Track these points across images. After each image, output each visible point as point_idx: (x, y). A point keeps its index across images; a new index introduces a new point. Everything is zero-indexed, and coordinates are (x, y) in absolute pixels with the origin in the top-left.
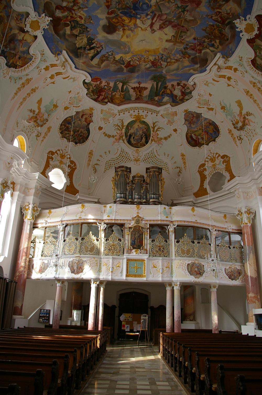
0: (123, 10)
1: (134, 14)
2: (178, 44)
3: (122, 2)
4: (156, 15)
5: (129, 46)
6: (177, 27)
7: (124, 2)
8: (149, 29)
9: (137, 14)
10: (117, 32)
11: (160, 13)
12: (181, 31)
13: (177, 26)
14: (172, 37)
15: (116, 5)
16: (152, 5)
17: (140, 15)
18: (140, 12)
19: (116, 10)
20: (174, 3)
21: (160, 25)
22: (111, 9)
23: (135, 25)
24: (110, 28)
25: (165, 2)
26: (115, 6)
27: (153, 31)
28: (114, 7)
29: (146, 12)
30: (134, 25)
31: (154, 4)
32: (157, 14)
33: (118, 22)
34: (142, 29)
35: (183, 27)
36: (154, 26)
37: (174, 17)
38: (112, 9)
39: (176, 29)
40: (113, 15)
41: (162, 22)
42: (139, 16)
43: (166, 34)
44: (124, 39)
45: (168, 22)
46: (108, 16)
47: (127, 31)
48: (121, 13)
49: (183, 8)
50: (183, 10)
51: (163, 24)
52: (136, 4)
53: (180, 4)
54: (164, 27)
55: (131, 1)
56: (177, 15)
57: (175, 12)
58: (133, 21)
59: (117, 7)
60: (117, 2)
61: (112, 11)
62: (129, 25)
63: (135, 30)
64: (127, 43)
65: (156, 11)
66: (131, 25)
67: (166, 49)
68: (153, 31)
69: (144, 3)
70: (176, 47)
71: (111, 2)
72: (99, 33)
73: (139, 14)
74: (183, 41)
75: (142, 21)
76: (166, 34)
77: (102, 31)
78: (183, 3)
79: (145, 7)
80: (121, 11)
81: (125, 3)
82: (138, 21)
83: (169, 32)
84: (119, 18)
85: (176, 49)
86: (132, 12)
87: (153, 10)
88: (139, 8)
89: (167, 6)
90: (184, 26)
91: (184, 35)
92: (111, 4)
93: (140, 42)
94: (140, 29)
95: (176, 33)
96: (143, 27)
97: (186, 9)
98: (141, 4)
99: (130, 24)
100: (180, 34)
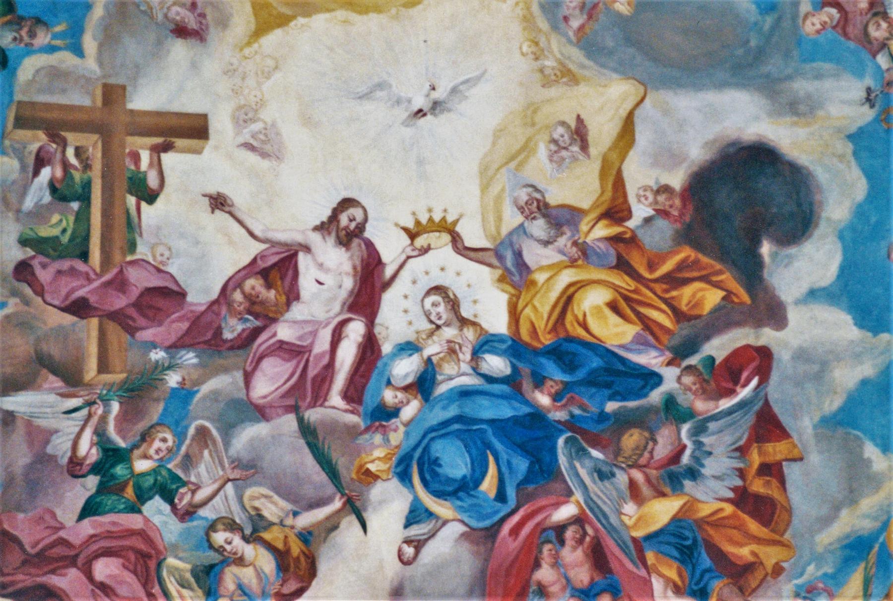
0: (632, 404)
1: (539, 382)
2: (78, 98)
3: (648, 480)
4: (346, 396)
5: (555, 28)
6: (135, 293)
7: (632, 484)
8: (390, 246)
9: (513, 381)
10: (677, 180)
11: (313, 415)
12: (84, 256)
13: (137, 305)
14: (153, 181)
15: (699, 444)
16: (395, 483)
17: (489, 379)
18: (488, 410)
19: (701, 405)
20: (212, 527)
21: (293, 295)
22: (742, 405)
23: (516, 275)
24: (743, 202)
25: (289, 521)
26: (705, 440)
27: (344, 224)
28: (712, 426)
29: (439, 415)
30: (522, 266)
31: (377, 491)
32: (336, 399)
33: (674, 280)
34: (456, 239)
35: (79, 308)
36: (349, 283)
37: (184, 394)
38: (730, 412)
39: (140, 279)
40: (719, 347)
41: (284, 332)
42: (496, 364)
43: (219, 202)
44: (604, 99)
45: (228, 335)
46: (767, 336)
47: (585, 205)
48: (652, 379)
49: (122, 487)
50: (120, 470)
51: (267, 316)
52: (526, 480)
53: (156, 520)
54: (254, 284)
55: (578, 496)
56: (156, 412)
57: (180, 436)
58: (540, 309)
59: (685, 428)
60: (693, 474)
61: (731, 392)
62: (573, 263)
63: (512, 219)
64: (576, 54)
65: (353, 432)
66: (557, 268)
67: (181, 31)
68: (344, 224)
69: (460, 490)
70: (90, 64)
71: (742, 473)
72: (849, 147)
73: (497, 388)
74: (36, 140)
75: (464, 322)
76: (219, 202)
77: (821, 175)
78: (132, 533)
79: (455, 462)
80: (656, 396)
81: (622, 478)
82: (497, 321)
83: (192, 239)
84: (664, 319)
85: (90, 44)
86: (556, 397)
87: (378, 438)
88: (498, 446)
89: (264, 490)
90: (68, 319)
91: (39, 214)
92: (742, 451)
93: (454, 90)
94: (473, 236)
95: (132, 226)
96: (442, 263)
97: (92, 482)
98: (488, 485)
99: (567, 277)
100: (83, 217)
